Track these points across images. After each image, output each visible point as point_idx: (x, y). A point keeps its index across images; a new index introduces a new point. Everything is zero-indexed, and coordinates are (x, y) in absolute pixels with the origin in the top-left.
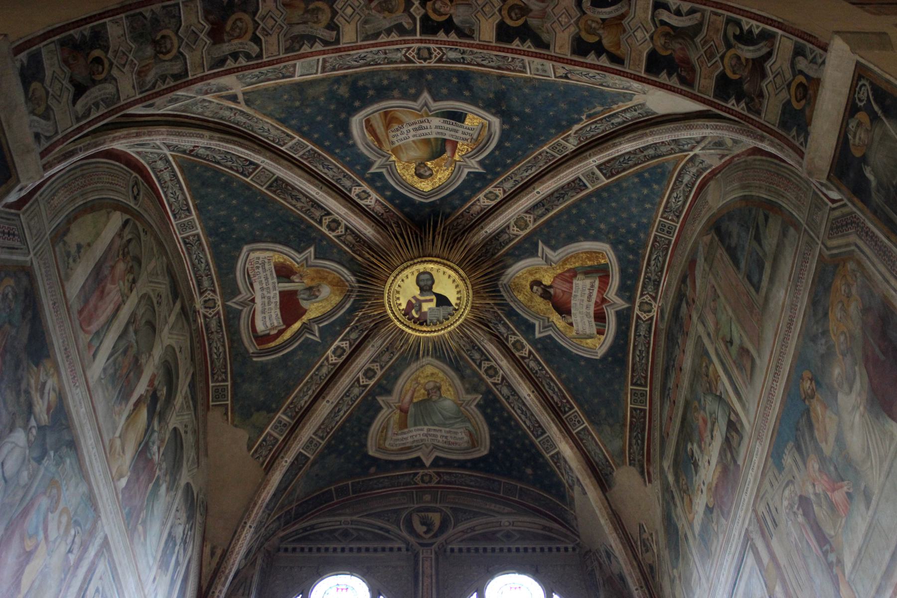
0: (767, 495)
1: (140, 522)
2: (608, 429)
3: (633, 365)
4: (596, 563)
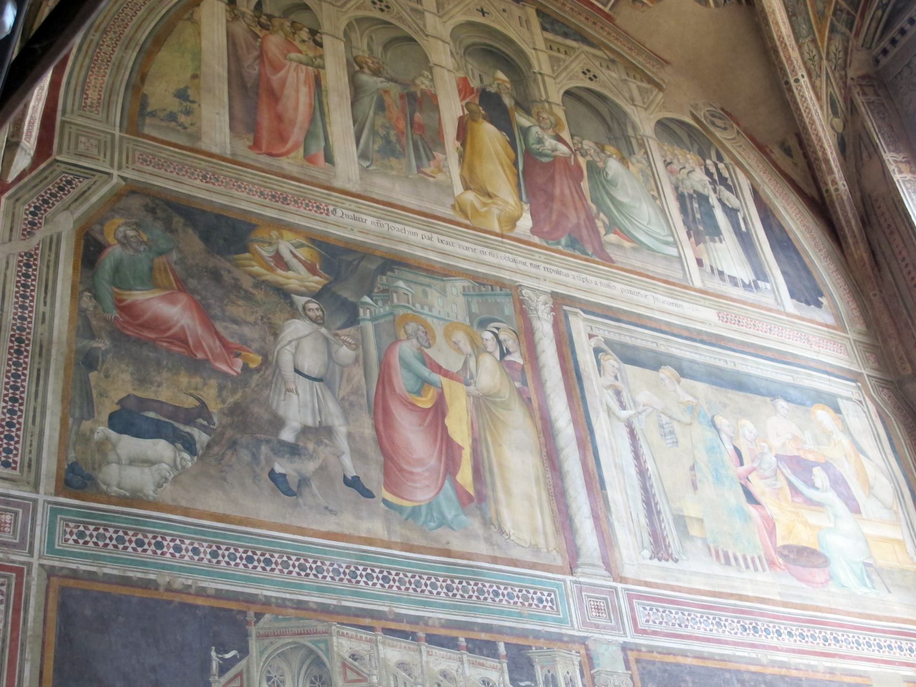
1: (602, 231)
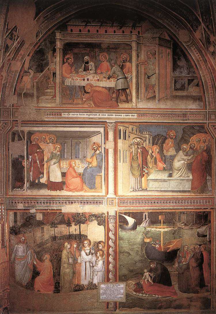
0: (128, 129)
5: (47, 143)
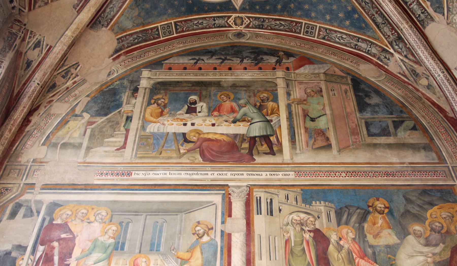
0: (276, 196)
2: (137, 13)
3: (190, 20)
4: (21, 35)
5: (89, 223)
